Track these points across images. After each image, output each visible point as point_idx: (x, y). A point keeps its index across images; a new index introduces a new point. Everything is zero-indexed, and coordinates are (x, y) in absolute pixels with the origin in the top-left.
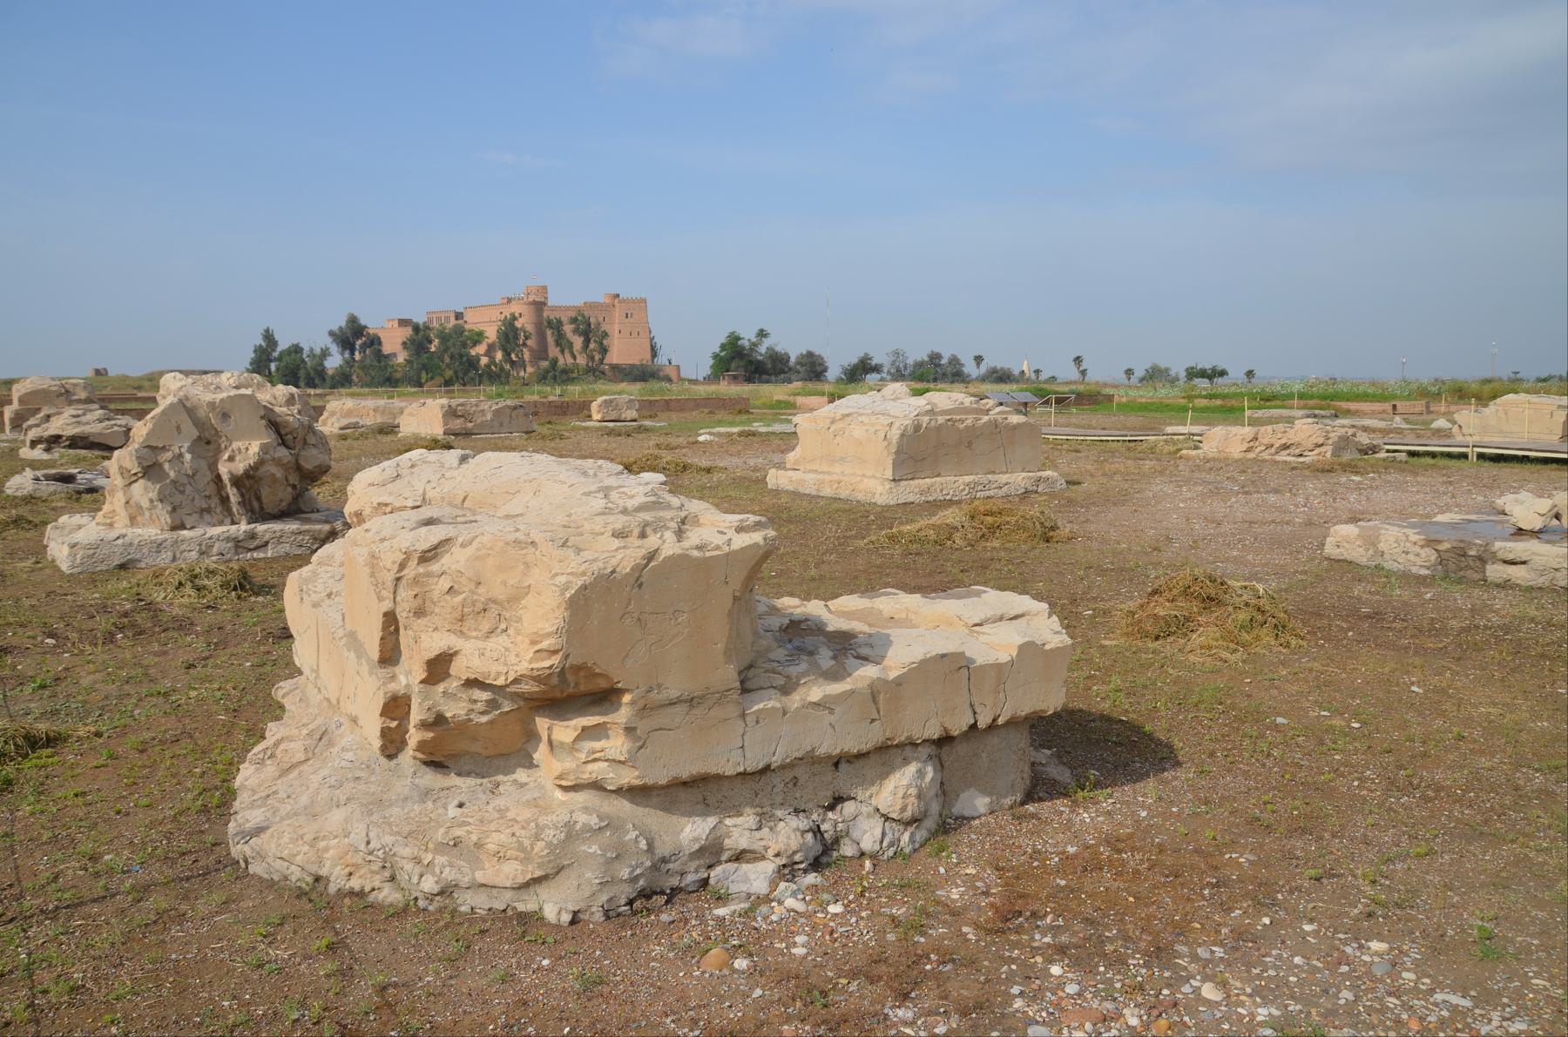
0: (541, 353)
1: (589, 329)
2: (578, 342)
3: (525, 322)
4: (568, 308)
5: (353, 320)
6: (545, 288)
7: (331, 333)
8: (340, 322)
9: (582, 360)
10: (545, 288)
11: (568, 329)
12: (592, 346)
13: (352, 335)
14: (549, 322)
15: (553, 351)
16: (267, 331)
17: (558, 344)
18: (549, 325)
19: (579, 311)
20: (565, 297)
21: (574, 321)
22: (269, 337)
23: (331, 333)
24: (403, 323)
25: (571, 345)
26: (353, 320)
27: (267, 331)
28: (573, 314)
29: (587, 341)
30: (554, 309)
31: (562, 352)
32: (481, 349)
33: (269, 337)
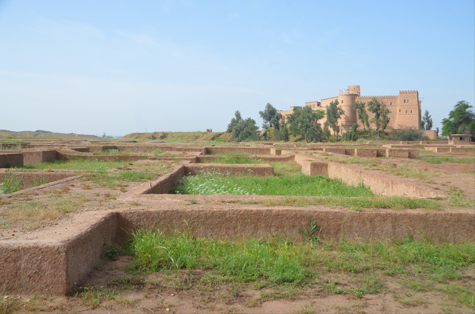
0: (352, 122)
1: (378, 107)
2: (372, 116)
3: (344, 106)
4: (370, 98)
5: (269, 106)
6: (358, 87)
7: (261, 113)
8: (263, 109)
9: (374, 127)
10: (358, 87)
11: (366, 108)
12: (381, 117)
13: (271, 114)
14: (357, 105)
15: (359, 122)
16: (237, 112)
17: (361, 117)
18: (357, 107)
19: (375, 99)
20: (368, 92)
21: (371, 103)
22: (238, 115)
23: (261, 113)
24: (291, 107)
25: (367, 117)
26: (269, 106)
27: (237, 112)
28: (370, 100)
29: (378, 116)
30: (363, 98)
31: (363, 122)
32: (322, 122)
33: (238, 115)
